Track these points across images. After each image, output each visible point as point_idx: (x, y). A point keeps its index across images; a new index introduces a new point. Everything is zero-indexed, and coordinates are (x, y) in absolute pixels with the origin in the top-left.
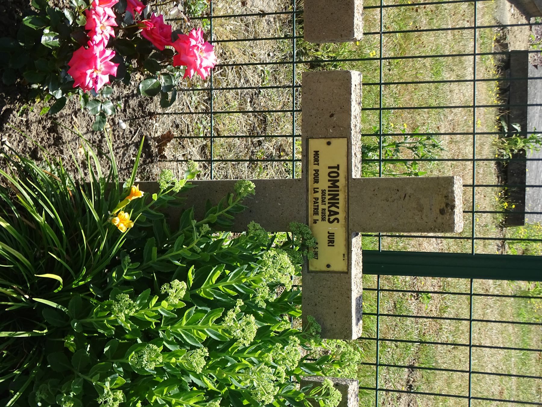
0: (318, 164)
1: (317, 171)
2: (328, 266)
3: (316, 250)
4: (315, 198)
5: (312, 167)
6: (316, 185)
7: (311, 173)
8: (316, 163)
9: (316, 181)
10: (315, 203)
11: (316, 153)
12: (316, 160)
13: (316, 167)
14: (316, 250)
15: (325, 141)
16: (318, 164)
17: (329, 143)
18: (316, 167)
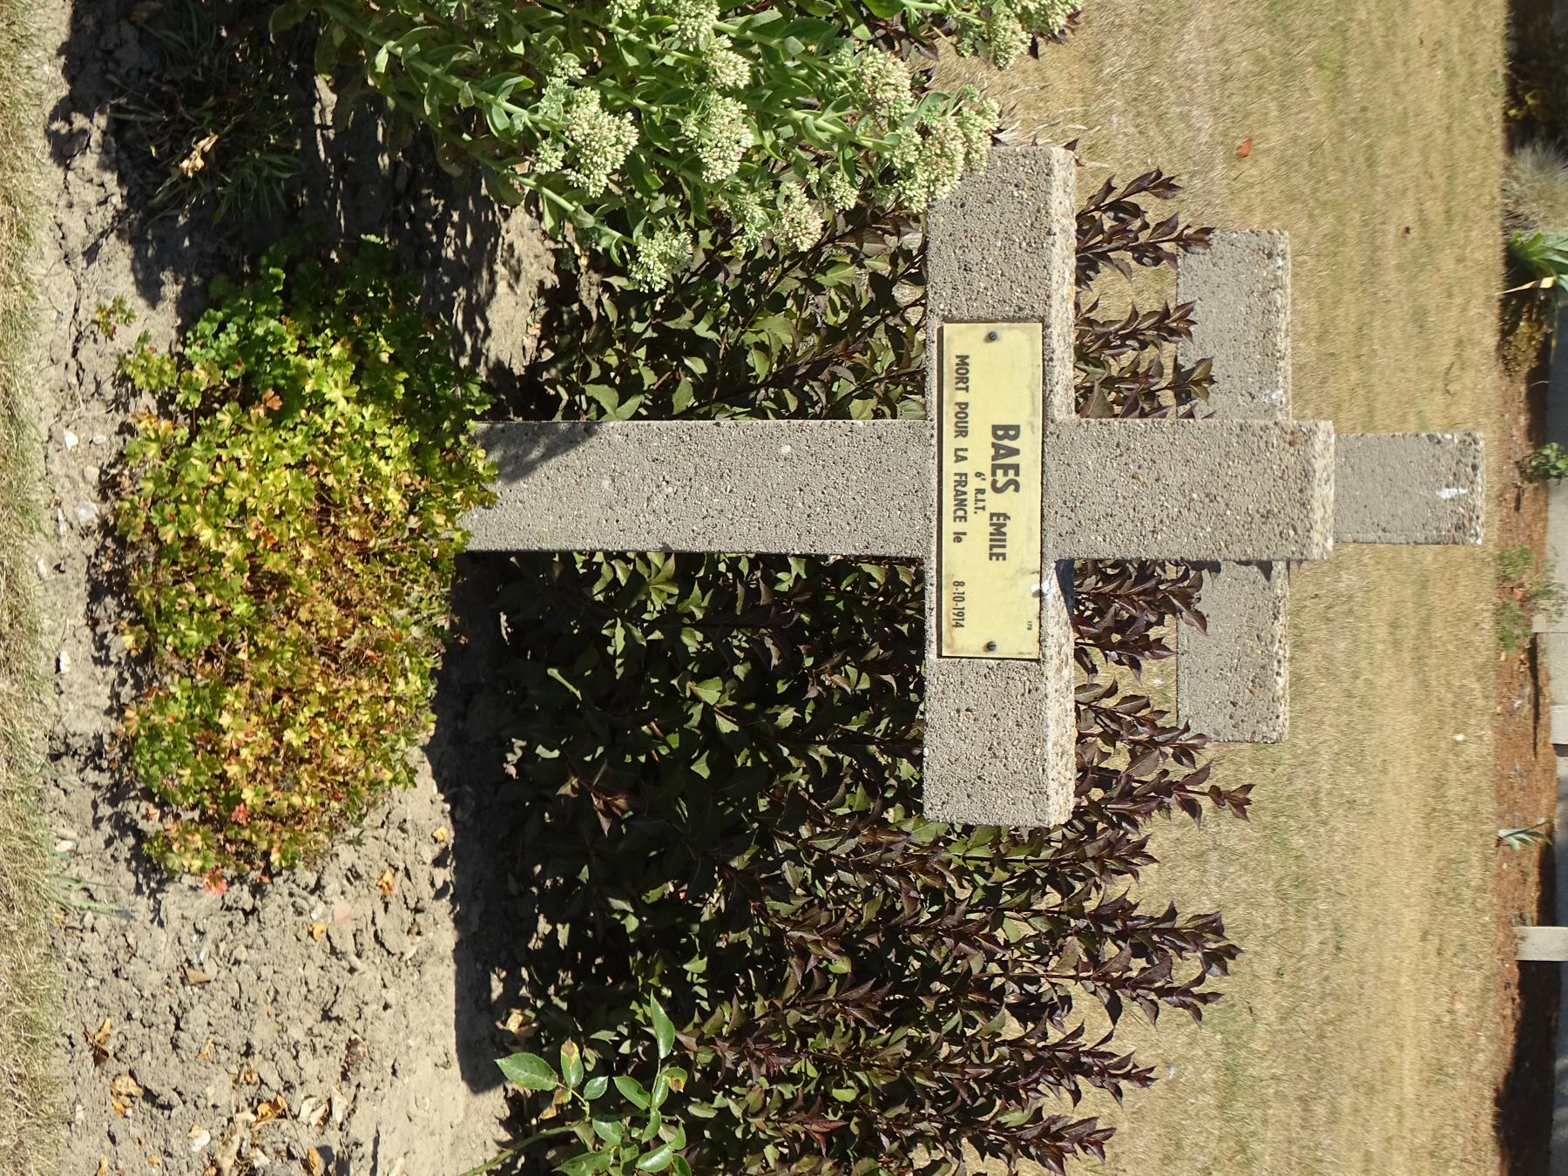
0: (967, 389)
1: (963, 407)
2: (990, 647)
3: (960, 605)
4: (961, 475)
5: (952, 396)
6: (962, 442)
7: (949, 412)
8: (961, 385)
9: (962, 432)
10: (959, 483)
11: (963, 361)
12: (963, 379)
13: (961, 397)
14: (960, 605)
15: (984, 329)
16: (967, 389)
17: (991, 337)
18: (961, 397)
